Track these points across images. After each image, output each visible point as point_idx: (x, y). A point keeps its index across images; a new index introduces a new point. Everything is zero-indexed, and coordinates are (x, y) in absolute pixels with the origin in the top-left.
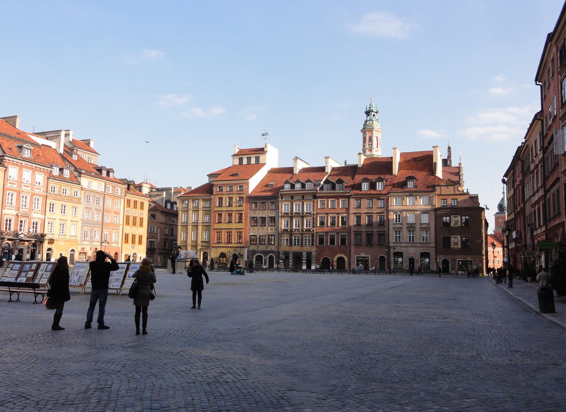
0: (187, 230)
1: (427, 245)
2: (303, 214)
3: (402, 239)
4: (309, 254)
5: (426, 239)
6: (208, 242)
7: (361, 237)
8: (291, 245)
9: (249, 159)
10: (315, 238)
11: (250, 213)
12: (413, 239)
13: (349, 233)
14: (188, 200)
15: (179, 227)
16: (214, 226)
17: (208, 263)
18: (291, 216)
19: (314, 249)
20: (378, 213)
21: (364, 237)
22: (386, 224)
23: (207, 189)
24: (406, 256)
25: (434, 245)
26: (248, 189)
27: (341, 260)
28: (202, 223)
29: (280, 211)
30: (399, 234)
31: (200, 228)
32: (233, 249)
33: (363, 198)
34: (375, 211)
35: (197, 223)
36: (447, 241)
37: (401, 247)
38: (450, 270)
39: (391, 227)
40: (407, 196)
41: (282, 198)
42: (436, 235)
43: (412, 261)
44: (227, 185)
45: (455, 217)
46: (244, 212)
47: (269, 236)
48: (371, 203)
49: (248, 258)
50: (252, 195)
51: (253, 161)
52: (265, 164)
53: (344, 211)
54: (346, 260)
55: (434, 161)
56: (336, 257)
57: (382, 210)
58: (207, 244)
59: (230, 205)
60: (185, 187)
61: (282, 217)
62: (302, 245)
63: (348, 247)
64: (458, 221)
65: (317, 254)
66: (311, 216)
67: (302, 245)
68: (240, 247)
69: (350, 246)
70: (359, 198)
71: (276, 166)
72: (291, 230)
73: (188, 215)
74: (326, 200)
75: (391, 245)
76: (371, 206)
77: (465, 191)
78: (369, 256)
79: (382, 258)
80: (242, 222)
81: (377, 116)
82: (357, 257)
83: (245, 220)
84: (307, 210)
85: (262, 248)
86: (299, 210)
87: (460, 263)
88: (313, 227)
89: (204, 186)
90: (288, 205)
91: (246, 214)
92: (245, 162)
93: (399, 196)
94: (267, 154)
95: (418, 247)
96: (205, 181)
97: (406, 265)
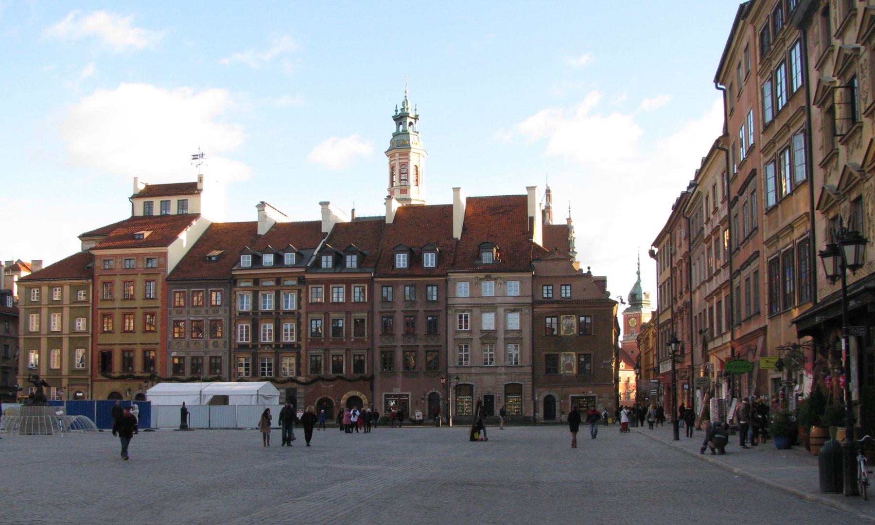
1: (517, 370)
2: (278, 313)
9: (165, 205)
10: (302, 361)
11: (170, 313)
13: (371, 350)
18: (255, 317)
25: (529, 370)
26: (165, 265)
29: (233, 309)
36: (552, 362)
37: (470, 374)
38: (557, 414)
40: (481, 279)
42: (533, 352)
45: (567, 318)
55: (529, 215)
56: (345, 397)
60: (27, 260)
64: (572, 326)
72: (255, 347)
75: (451, 371)
77: (585, 271)
78: (410, 393)
81: (417, 126)
88: (299, 339)
93: (466, 280)
94: (203, 194)
96: (76, 247)
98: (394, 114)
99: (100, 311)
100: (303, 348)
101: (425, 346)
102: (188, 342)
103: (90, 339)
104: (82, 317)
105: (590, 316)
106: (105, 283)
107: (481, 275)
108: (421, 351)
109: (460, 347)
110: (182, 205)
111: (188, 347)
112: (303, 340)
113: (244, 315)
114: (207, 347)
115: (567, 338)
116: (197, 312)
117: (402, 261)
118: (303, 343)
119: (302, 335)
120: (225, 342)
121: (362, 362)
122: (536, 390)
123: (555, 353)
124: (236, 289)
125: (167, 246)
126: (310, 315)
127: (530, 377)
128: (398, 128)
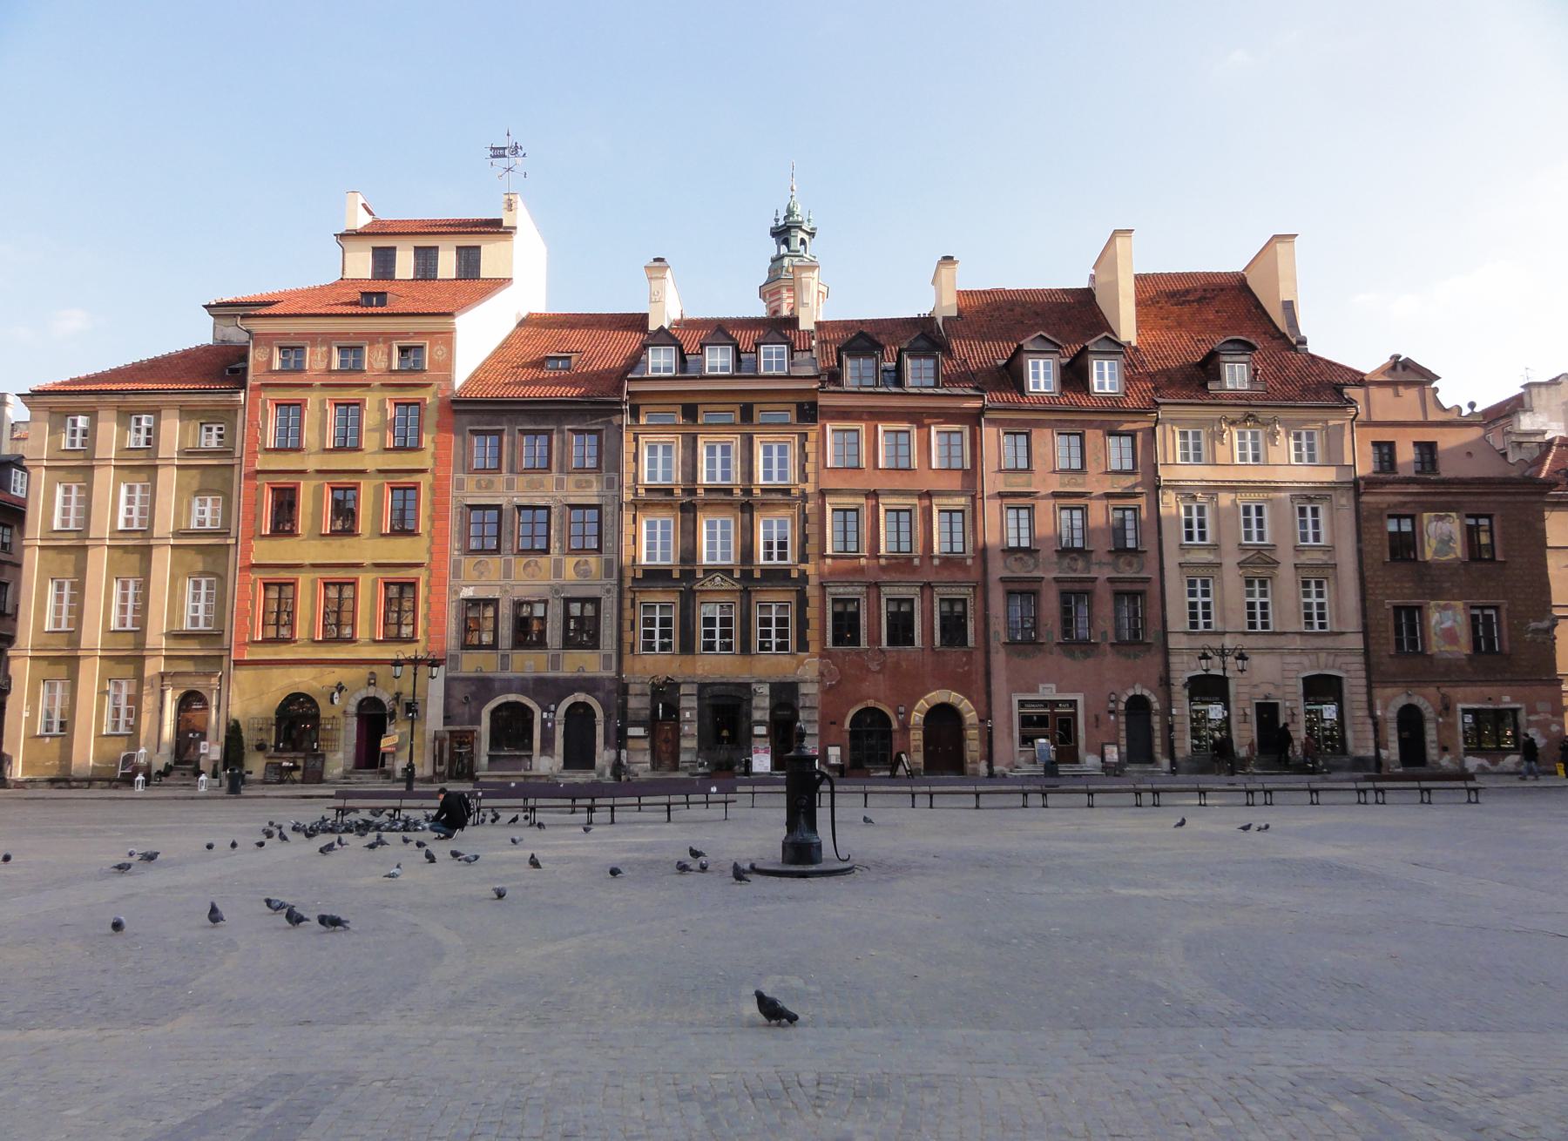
0: (81, 571)
1: (1328, 642)
2: (748, 492)
3: (1223, 619)
4: (785, 695)
5: (1321, 616)
6: (212, 637)
7: (1037, 606)
8: (687, 647)
9: (426, 257)
10: (812, 612)
11: (460, 485)
12: (1264, 616)
13: (982, 587)
14: (92, 414)
15: (32, 561)
16: (248, 551)
17: (211, 750)
18: (686, 504)
19: (807, 670)
20: (1109, 496)
21: (1050, 603)
22: (1150, 546)
23: (215, 372)
24: (1244, 693)
25: (1357, 642)
26: (448, 365)
27: (944, 720)
28: (178, 534)
29: (627, 479)
30: (1206, 593)
31: (163, 562)
32: (364, 671)
33: (1039, 424)
34: (1095, 484)
35: (147, 533)
38: (1432, 752)
39: (1171, 560)
40: (1233, 423)
41: (635, 413)
42: (1363, 599)
43: (1267, 712)
44: (326, 339)
45: (1440, 519)
46: (425, 481)
47: (568, 601)
48: (1076, 452)
49: (448, 718)
50: (476, 393)
51: (447, 265)
52: (506, 282)
53: (955, 482)
54: (971, 716)
56: (923, 705)
57: (1129, 481)
58: (208, 649)
61: (637, 505)
62: (746, 648)
63: (979, 657)
64: (1451, 538)
65: (826, 691)
66: (788, 505)
67: (746, 648)
68: (415, 662)
69: (987, 653)
70: (1022, 424)
71: (540, 307)
73: (87, 490)
74: (862, 426)
75: (1173, 642)
76: (1076, 464)
77: (1466, 411)
79: (1138, 706)
80: (412, 533)
82: (1022, 704)
83: (432, 519)
84: (768, 475)
85: (529, 664)
86: (726, 475)
87: (1469, 719)
88: (804, 558)
89: (186, 354)
90: (667, 449)
91: (439, 489)
92: (405, 265)
94: (516, 238)
95: (1292, 652)
96: (200, 333)
97: (1244, 736)
98: (773, 224)
100: (814, 580)
101: (1111, 580)
104: (210, 492)
105: (1489, 517)
107: (1237, 414)
108: (1104, 594)
109: (1192, 583)
111: (507, 575)
113: (659, 497)
114: (558, 574)
115: (1446, 565)
116: (532, 486)
117: (1041, 375)
119: (811, 549)
120: (609, 563)
121: (910, 616)
122: (1377, 692)
123: (1415, 602)
124: (638, 430)
125: (450, 315)
126: (828, 500)
127: (1361, 659)
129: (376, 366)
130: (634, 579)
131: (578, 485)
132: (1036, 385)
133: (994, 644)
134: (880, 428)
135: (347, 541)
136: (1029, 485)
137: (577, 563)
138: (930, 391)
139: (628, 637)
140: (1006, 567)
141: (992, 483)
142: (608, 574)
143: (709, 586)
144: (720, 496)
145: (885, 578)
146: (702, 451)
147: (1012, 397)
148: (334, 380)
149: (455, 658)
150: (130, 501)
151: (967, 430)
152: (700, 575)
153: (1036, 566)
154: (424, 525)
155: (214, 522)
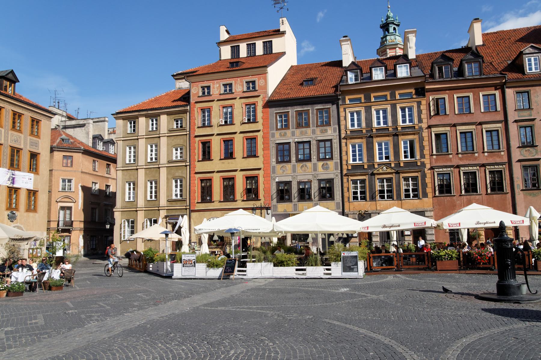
9: (251, 48)
10: (428, 180)
11: (273, 135)
26: (265, 87)
29: (342, 127)
46: (260, 135)
50: (277, 98)
51: (260, 50)
52: (283, 54)
59: (229, 121)
80: (255, 156)
88: (423, 156)
92: (243, 52)
99: (197, 139)
102: (294, 166)
103: (188, 167)
106: (203, 110)
110: (268, 46)
111: (294, 170)
112: (427, 157)
114: (315, 169)
116: (302, 133)
118: (427, 161)
119: (426, 152)
120: (336, 163)
125: (266, 67)
128: (384, 33)
129: (237, 90)
130: (348, 169)
131: (322, 132)
132: (530, 69)
133: (517, 191)
134: (455, 96)
135: (230, 161)
136: (531, 116)
137: (323, 165)
138: (478, 77)
139: (346, 195)
140: (521, 154)
141: (512, 116)
142: (336, 169)
143: (381, 171)
144: (382, 132)
145: (461, 163)
146: (374, 113)
147: (520, 76)
148: (222, 97)
149: (275, 207)
150: (152, 151)
151: (497, 93)
152: (376, 166)
153: (537, 153)
154: (260, 152)
155: (181, 157)
